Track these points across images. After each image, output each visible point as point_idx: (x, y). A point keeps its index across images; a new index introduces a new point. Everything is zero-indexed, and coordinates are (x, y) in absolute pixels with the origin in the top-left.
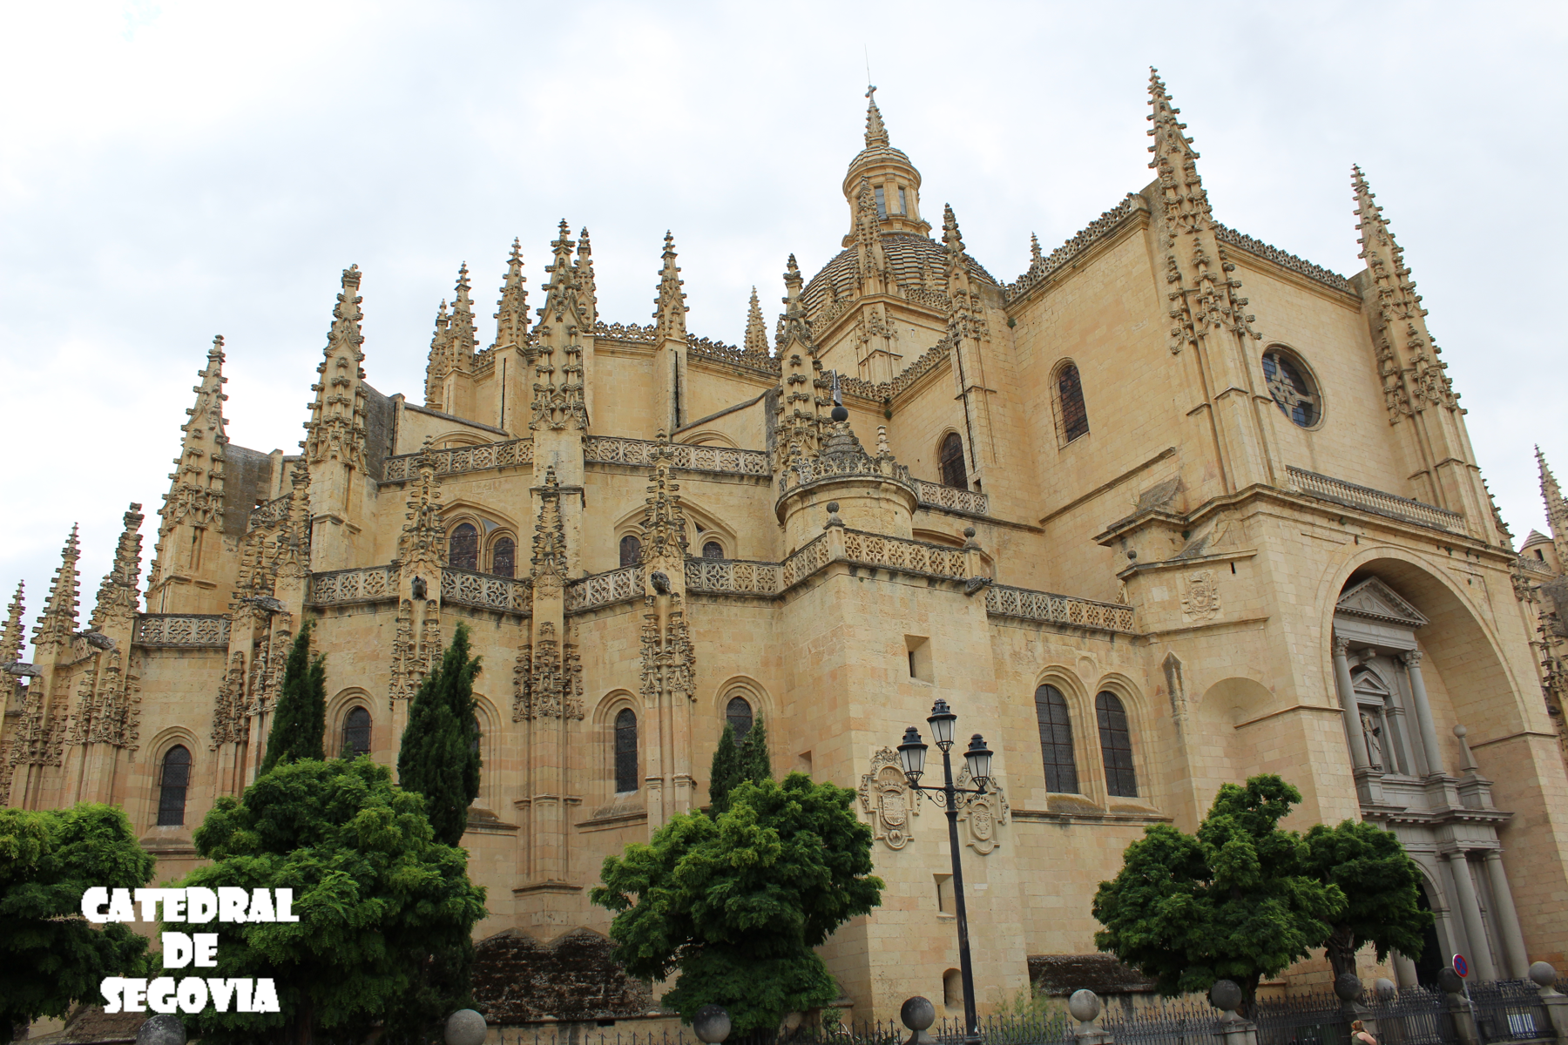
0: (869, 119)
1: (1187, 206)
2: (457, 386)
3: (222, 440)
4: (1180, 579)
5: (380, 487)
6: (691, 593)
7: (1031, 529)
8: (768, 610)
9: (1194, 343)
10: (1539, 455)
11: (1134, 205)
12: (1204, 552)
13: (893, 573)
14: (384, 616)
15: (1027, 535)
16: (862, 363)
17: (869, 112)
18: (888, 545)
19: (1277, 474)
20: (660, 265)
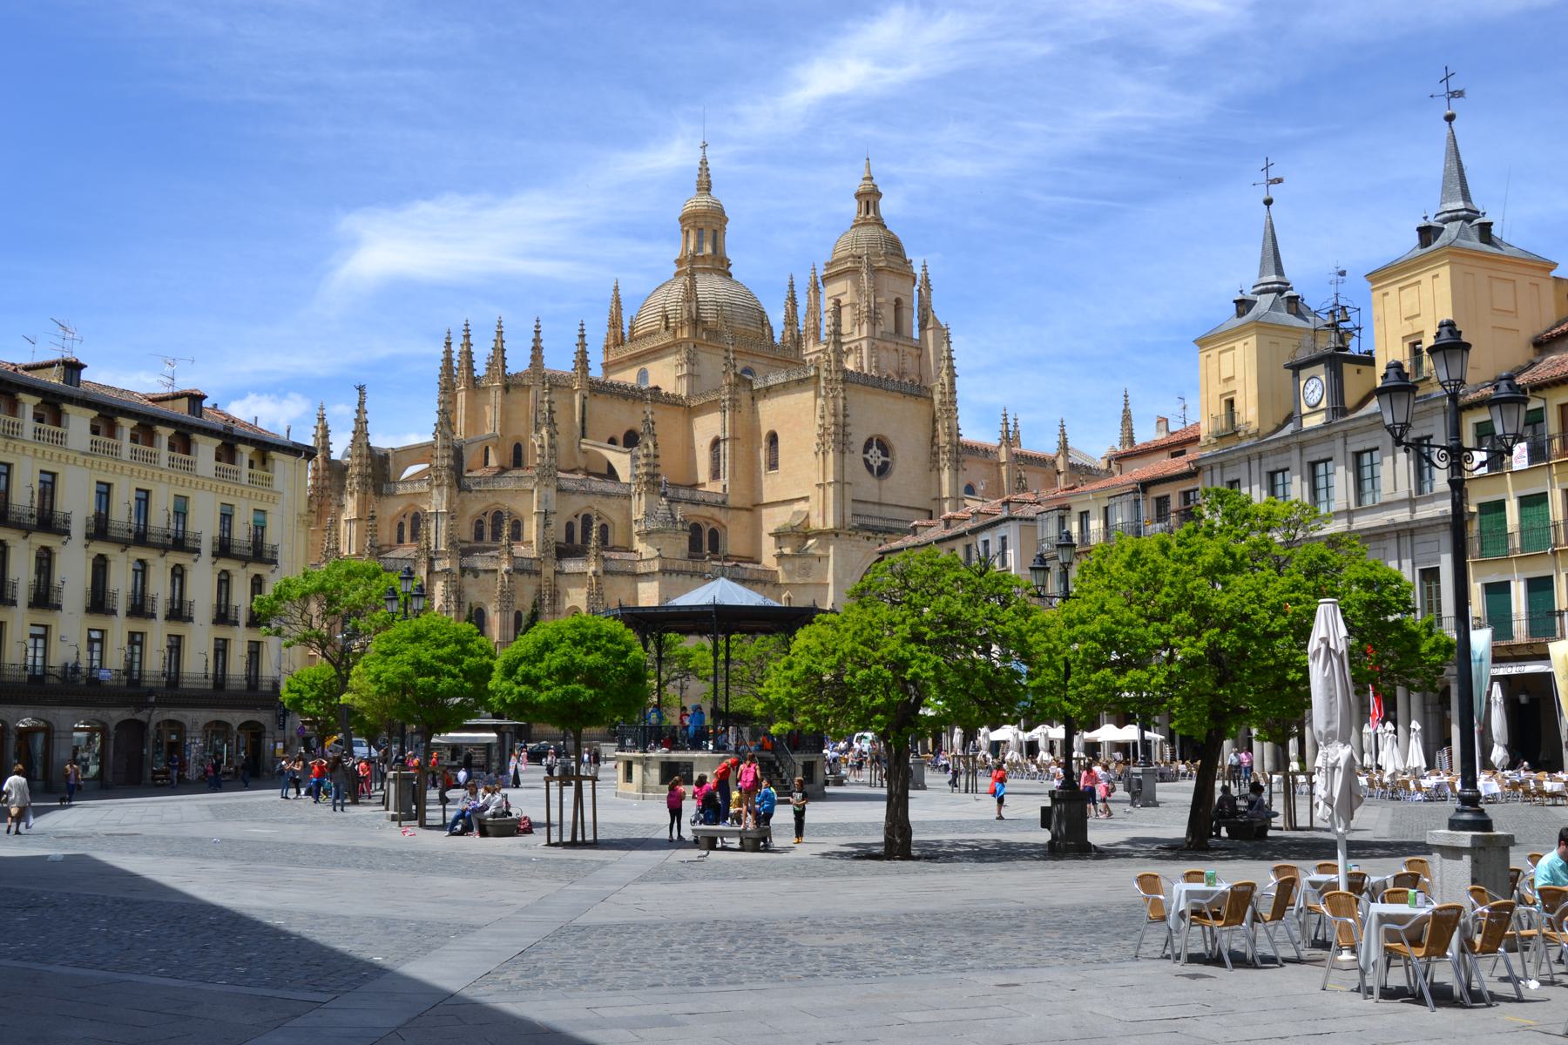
0: (700, 169)
1: (833, 382)
2: (466, 396)
3: (368, 444)
4: (798, 561)
5: (459, 491)
6: (606, 572)
7: (747, 510)
8: (631, 578)
9: (823, 453)
10: (1126, 396)
11: (812, 373)
12: (809, 551)
13: (679, 572)
14: (489, 576)
15: (745, 513)
16: (679, 377)
17: (701, 163)
18: (677, 562)
19: (846, 519)
20: (577, 340)
